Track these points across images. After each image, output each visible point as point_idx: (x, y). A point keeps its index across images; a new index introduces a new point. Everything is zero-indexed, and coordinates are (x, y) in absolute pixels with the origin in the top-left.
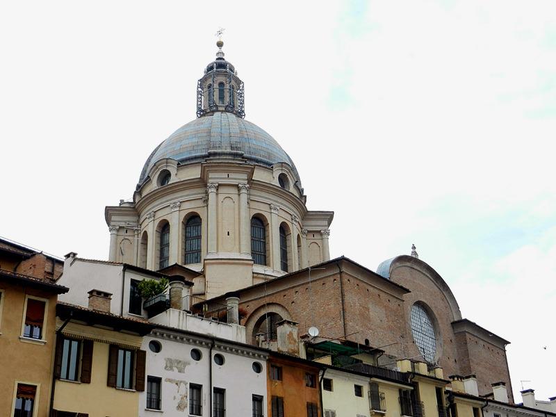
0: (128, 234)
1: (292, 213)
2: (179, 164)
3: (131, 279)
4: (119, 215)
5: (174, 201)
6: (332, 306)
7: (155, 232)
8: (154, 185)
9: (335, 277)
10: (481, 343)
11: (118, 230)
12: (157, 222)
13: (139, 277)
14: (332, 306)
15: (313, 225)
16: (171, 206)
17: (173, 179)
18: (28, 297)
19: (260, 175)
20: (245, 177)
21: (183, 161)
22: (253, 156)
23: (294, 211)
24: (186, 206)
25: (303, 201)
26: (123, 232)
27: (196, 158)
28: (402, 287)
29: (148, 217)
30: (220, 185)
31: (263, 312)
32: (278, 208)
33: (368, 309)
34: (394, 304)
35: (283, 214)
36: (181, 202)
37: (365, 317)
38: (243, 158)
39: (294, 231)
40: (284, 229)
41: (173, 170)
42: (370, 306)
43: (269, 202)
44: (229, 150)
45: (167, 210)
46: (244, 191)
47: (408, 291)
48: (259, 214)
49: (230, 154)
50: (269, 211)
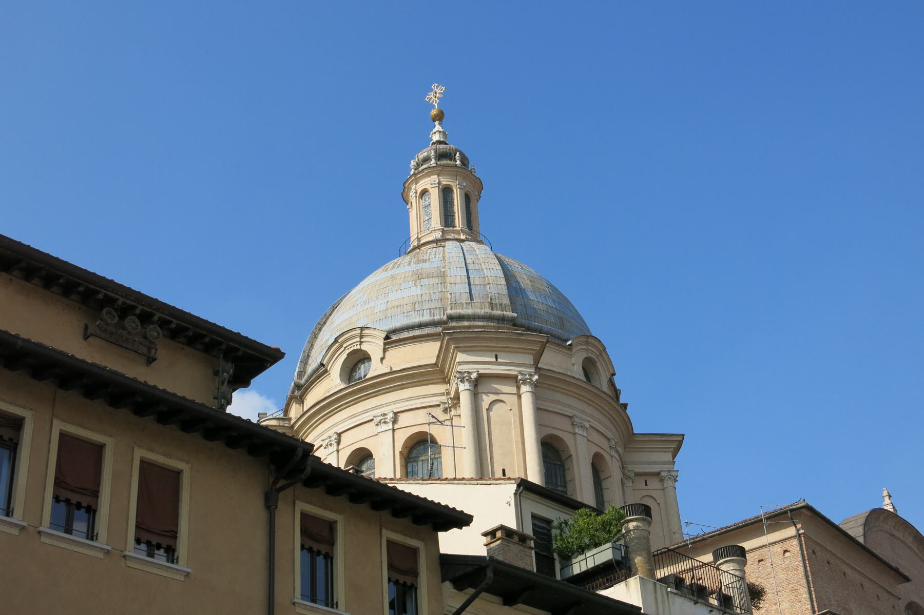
1: (610, 435)
2: (387, 337)
6: (785, 605)
8: (333, 382)
9: (786, 545)
15: (654, 460)
17: (375, 368)
18: (388, 534)
20: (529, 359)
21: (395, 331)
27: (421, 326)
28: (896, 571)
29: (324, 444)
30: (481, 376)
32: (587, 425)
36: (396, 414)
40: (597, 467)
43: (570, 412)
44: (487, 310)
45: (370, 429)
46: (525, 389)
47: (907, 580)
49: (490, 318)
50: (570, 429)
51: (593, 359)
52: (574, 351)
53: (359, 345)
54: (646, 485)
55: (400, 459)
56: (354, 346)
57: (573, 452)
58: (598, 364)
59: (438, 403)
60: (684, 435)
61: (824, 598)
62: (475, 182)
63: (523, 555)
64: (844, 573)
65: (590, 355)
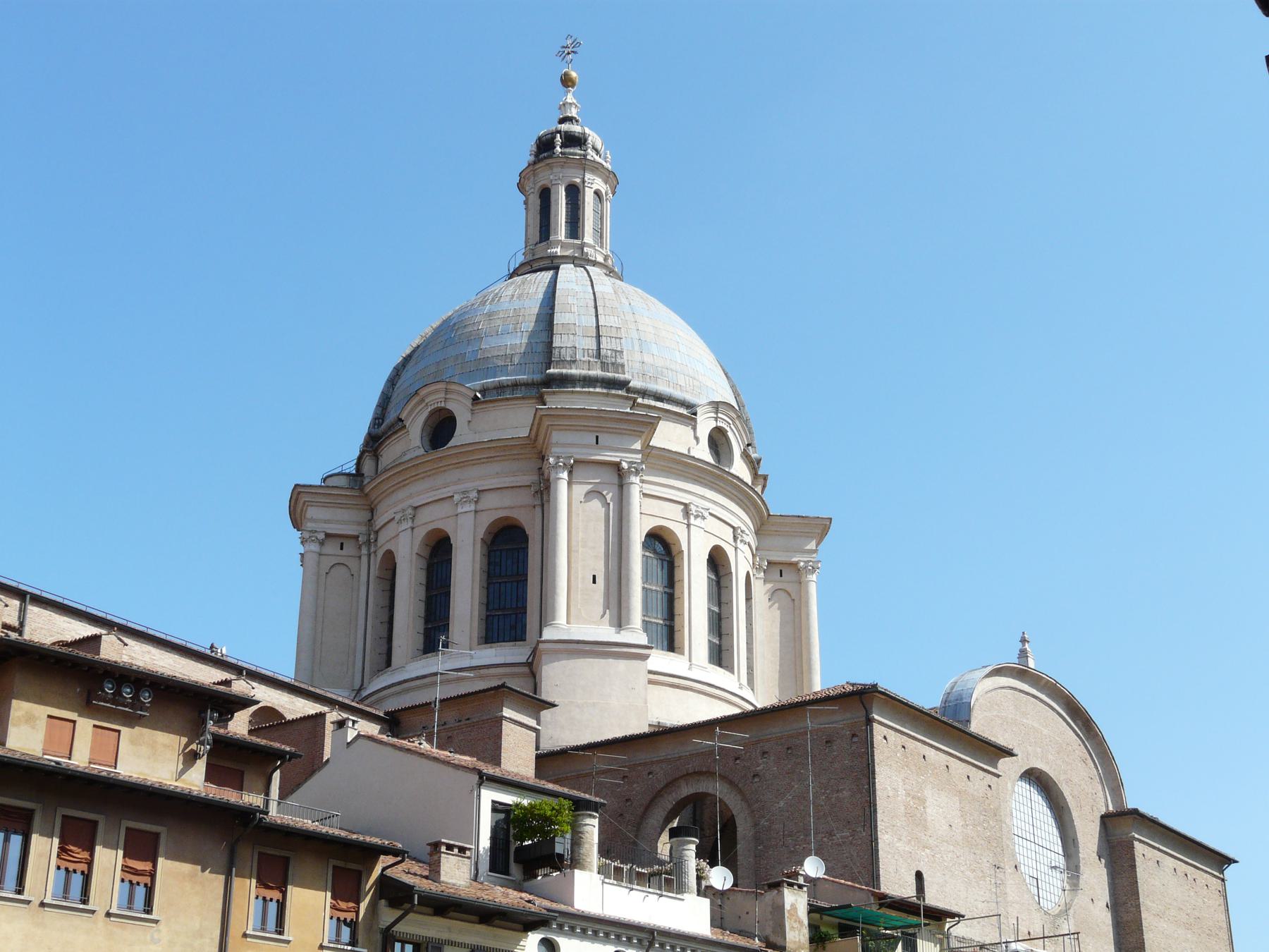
0: (344, 552)
3: (493, 802)
4: (324, 505)
5: (461, 487)
6: (846, 793)
7: (414, 556)
10: (1170, 862)
11: (322, 543)
12: (421, 533)
13: (508, 798)
14: (846, 793)
16: (457, 497)
17: (463, 435)
18: (333, 862)
19: (669, 436)
22: (652, 386)
23: (741, 518)
24: (490, 501)
25: (759, 489)
26: (332, 548)
29: (398, 517)
31: (686, 790)
32: (706, 514)
33: (922, 801)
34: (980, 780)
35: (711, 524)
36: (479, 492)
37: (915, 817)
38: (628, 390)
39: (741, 563)
40: (717, 561)
41: (461, 411)
42: (928, 793)
47: (1009, 753)
48: (661, 528)
51: (724, 428)
52: (699, 418)
53: (443, 403)
54: (781, 576)
55: (482, 547)
56: (438, 402)
57: (684, 547)
58: (730, 434)
59: (528, 484)
60: (831, 519)
61: (889, 789)
62: (608, 177)
63: (460, 864)
64: (924, 757)
65: (720, 424)
